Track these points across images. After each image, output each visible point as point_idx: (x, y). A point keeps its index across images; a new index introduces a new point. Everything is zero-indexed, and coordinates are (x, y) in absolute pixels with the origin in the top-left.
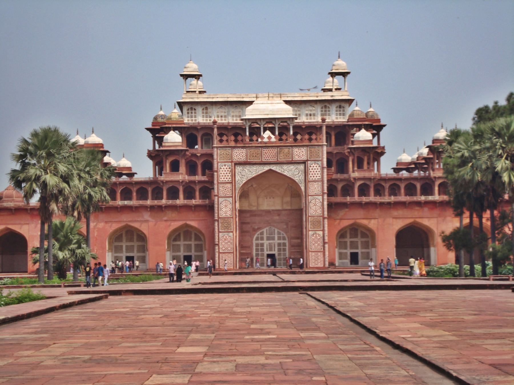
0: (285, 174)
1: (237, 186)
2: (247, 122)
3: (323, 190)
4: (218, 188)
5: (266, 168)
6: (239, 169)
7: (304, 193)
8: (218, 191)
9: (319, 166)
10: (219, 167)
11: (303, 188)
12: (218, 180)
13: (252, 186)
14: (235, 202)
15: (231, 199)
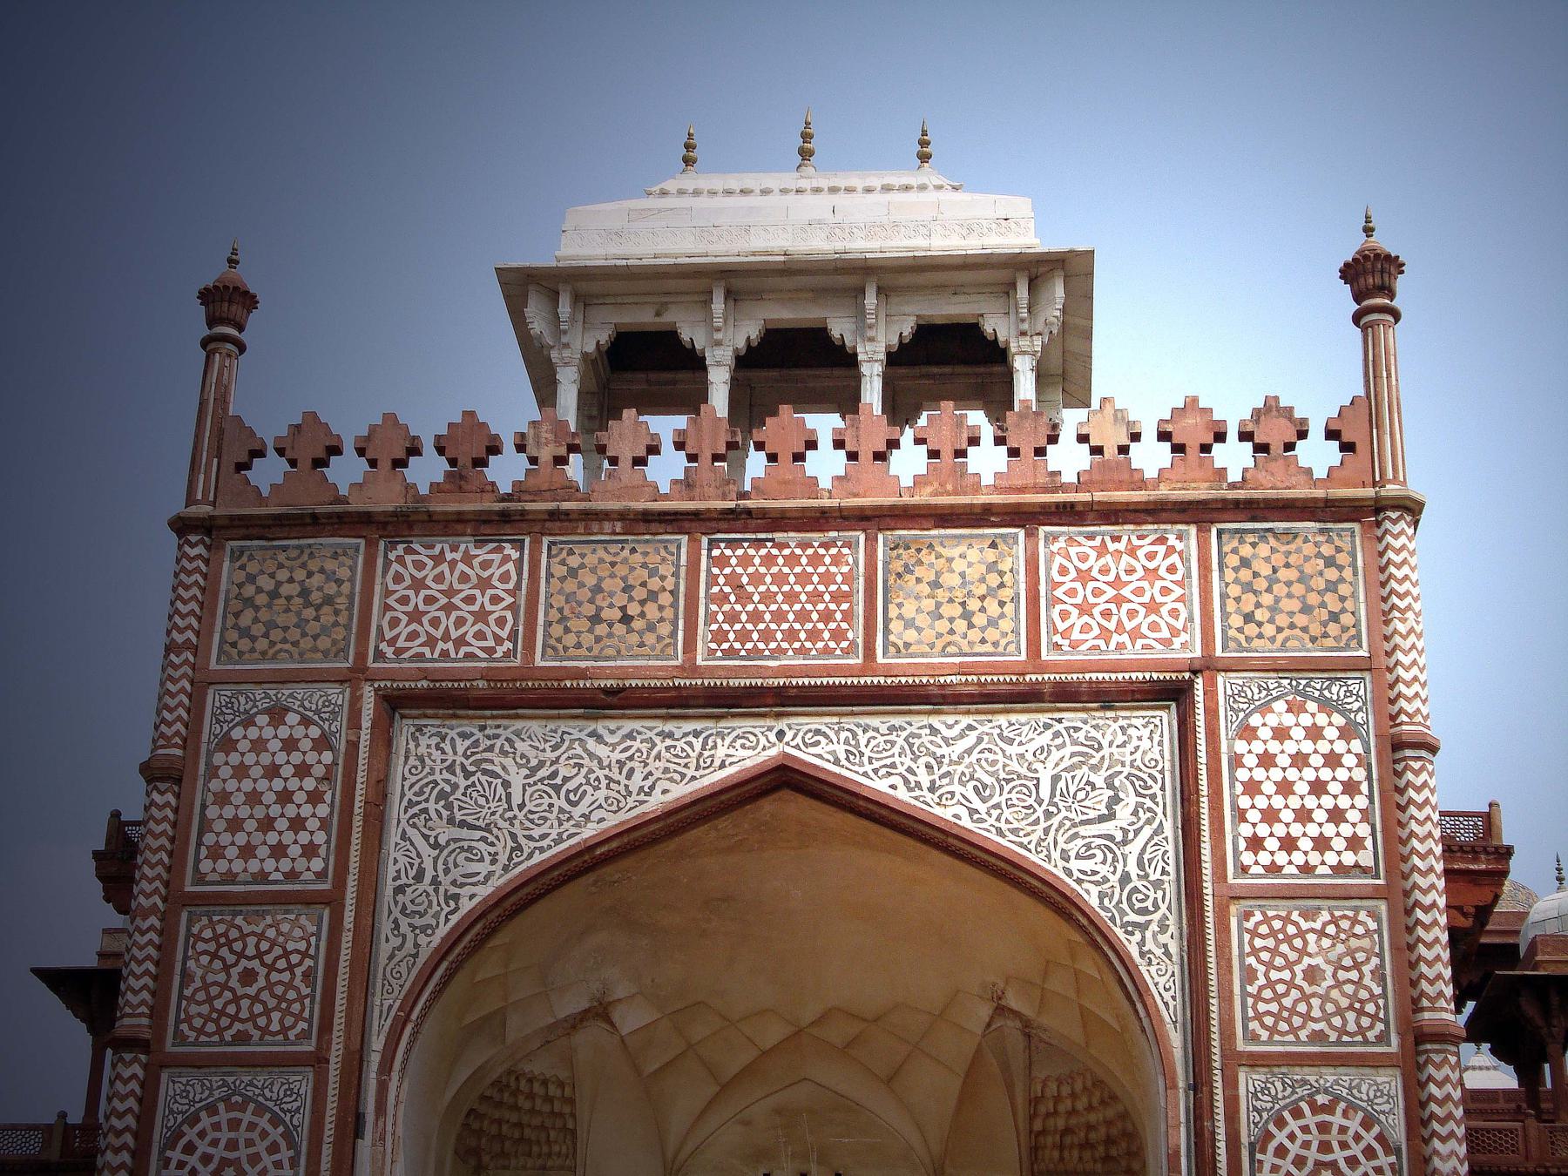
0: (946, 813)
1: (384, 949)
2: (565, 309)
3: (1412, 1003)
4: (164, 963)
5: (742, 748)
6: (428, 752)
7: (1176, 1039)
8: (160, 994)
9: (1346, 733)
10: (209, 729)
11: (1162, 980)
12: (175, 867)
13: (601, 1011)
14: (352, 1125)
15: (303, 1082)
